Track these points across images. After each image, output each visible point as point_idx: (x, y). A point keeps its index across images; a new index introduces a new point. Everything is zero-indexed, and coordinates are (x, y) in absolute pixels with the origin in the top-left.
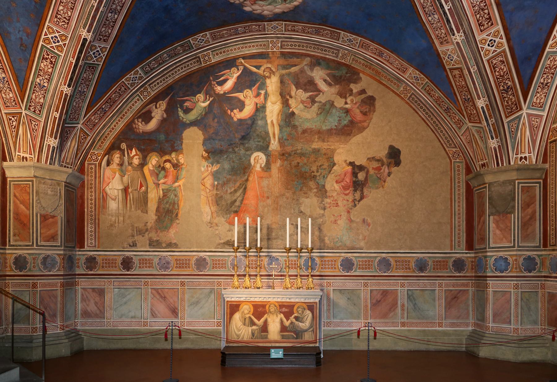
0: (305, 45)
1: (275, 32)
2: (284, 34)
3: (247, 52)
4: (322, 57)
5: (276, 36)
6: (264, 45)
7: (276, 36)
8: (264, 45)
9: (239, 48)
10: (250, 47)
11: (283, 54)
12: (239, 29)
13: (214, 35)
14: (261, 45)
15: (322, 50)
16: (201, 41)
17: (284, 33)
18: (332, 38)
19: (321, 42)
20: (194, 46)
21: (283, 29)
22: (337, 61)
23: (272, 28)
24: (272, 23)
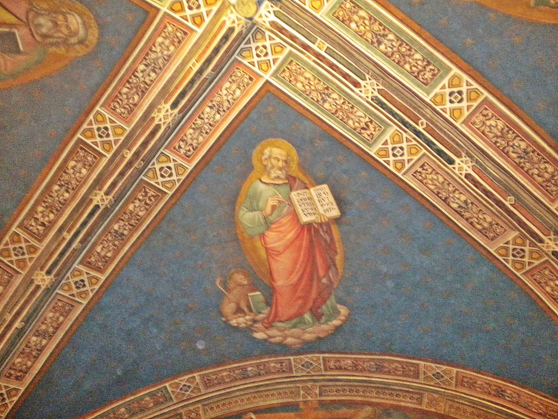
0: (361, 389)
1: (308, 372)
2: (324, 375)
3: (262, 403)
4: (392, 406)
5: (309, 378)
6: (292, 392)
7: (309, 378)
8: (292, 392)
9: (248, 399)
10: (267, 396)
11: (322, 404)
12: (250, 369)
13: (208, 379)
14: (286, 393)
15: (391, 394)
16: (185, 388)
17: (323, 373)
18: (405, 376)
19: (389, 384)
20: (173, 397)
21: (322, 367)
22: (420, 410)
23: (303, 365)
24: (302, 357)
